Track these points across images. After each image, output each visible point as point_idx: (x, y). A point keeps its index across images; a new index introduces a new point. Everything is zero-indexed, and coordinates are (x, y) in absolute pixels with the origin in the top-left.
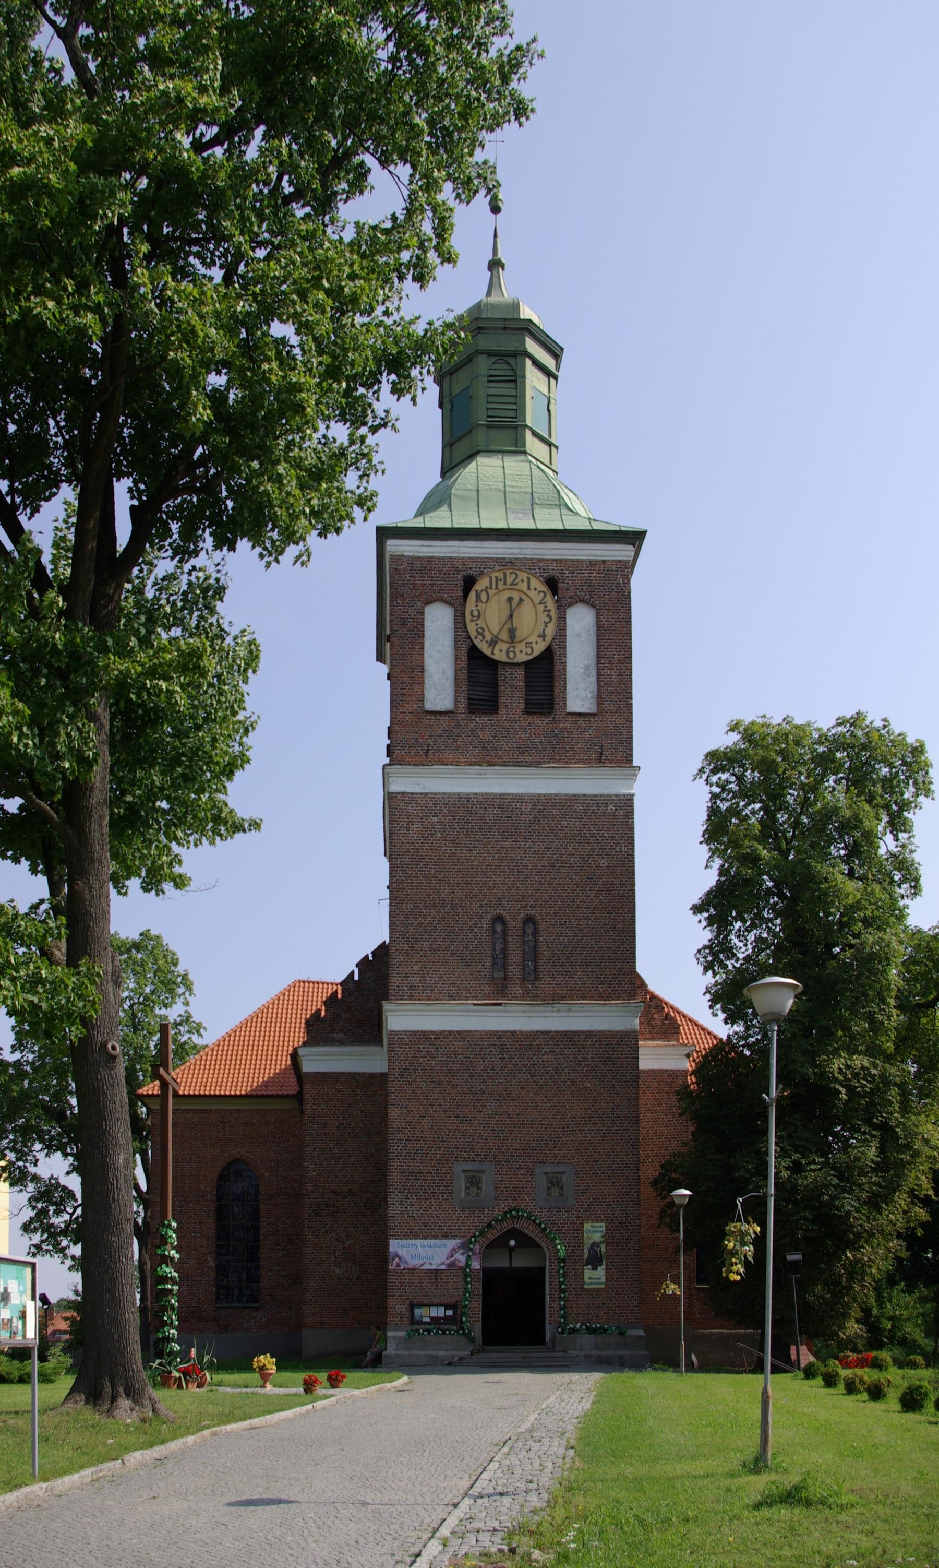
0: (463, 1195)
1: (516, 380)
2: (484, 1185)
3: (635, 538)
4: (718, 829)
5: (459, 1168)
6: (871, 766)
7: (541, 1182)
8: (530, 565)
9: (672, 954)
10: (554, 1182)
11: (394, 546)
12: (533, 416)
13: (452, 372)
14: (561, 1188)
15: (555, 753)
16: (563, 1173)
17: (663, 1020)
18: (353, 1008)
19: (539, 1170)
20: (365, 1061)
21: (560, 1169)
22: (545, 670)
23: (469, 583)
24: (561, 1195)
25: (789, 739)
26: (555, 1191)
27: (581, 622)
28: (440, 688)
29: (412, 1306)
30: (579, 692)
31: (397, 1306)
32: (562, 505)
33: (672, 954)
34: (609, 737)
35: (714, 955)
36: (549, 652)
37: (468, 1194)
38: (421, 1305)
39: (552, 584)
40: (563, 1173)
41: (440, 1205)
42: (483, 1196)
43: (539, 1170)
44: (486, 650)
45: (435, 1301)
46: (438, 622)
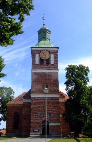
1: (46, 34)
3: (58, 48)
4: (67, 75)
6: (83, 70)
8: (48, 50)
9: (62, 88)
11: (32, 49)
12: (47, 37)
13: (40, 33)
15: (49, 68)
17: (62, 95)
18: (27, 95)
20: (29, 101)
22: (48, 61)
23: (40, 52)
25: (74, 67)
27: (52, 56)
28: (37, 61)
30: (52, 62)
31: (32, 130)
32: (50, 45)
33: (62, 88)
34: (55, 67)
35: (67, 89)
36: (49, 59)
39: (49, 52)
44: (42, 58)
46: (37, 56)
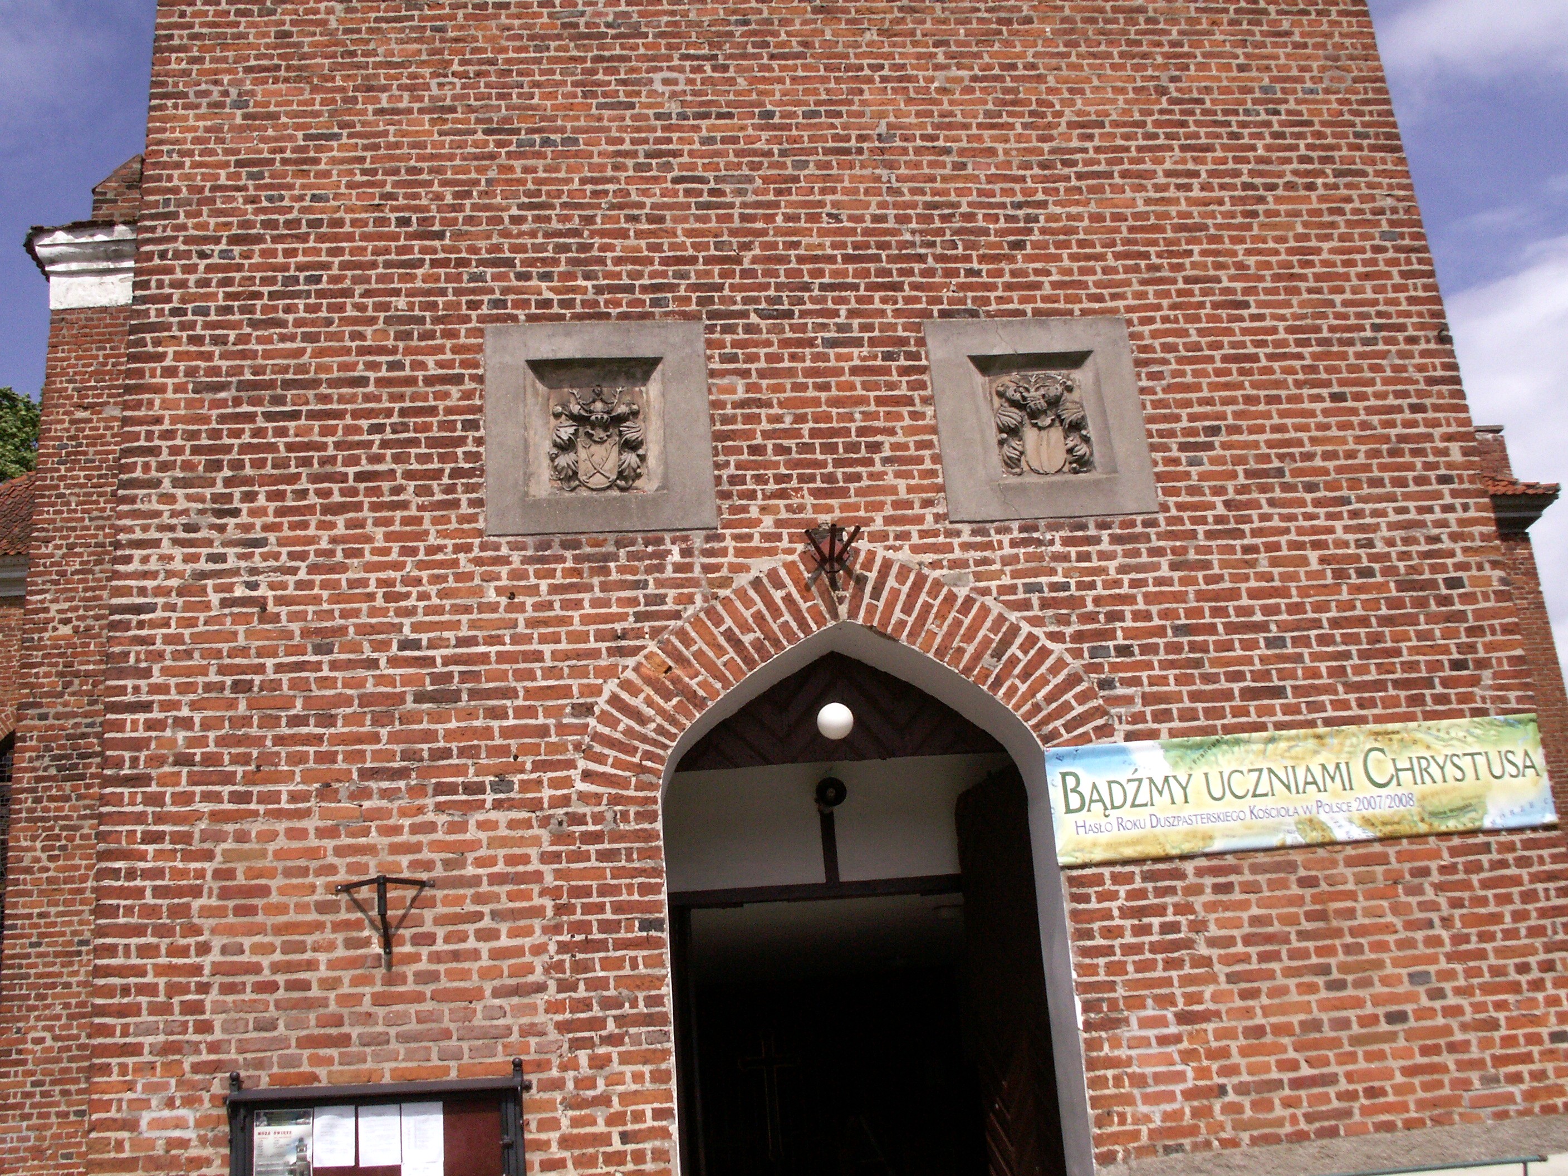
0: (543, 484)
2: (652, 433)
5: (508, 352)
7: (966, 408)
10: (1033, 391)
14: (1076, 427)
16: (1075, 360)
19: (948, 349)
21: (1054, 339)
24: (1082, 463)
26: (1045, 447)
29: (245, 1110)
37: (569, 477)
38: (298, 1104)
40: (1075, 360)
41: (409, 538)
42: (648, 485)
43: (948, 349)
45: (386, 1074)
